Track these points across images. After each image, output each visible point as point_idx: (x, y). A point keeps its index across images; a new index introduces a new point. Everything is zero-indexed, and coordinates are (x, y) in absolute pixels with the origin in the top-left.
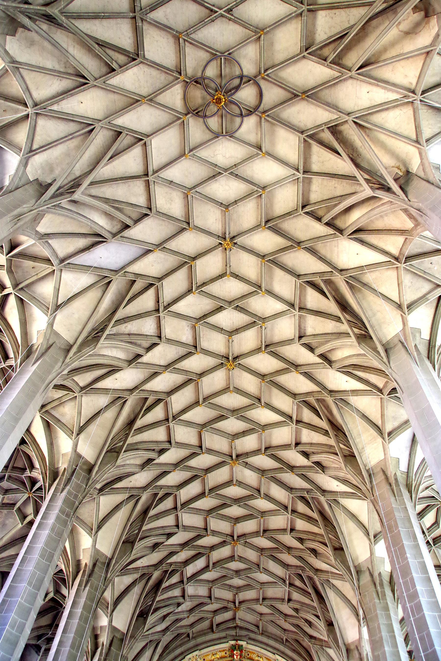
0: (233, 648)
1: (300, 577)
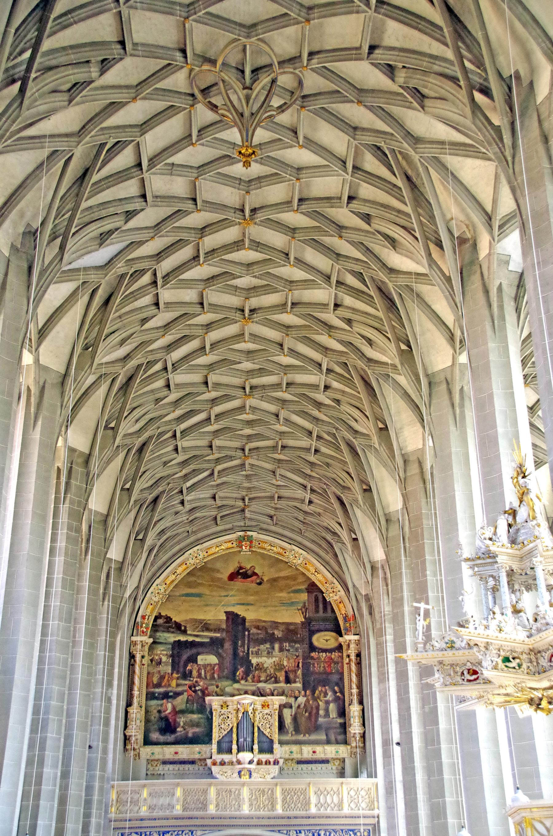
0: (240, 541)
1: (359, 276)
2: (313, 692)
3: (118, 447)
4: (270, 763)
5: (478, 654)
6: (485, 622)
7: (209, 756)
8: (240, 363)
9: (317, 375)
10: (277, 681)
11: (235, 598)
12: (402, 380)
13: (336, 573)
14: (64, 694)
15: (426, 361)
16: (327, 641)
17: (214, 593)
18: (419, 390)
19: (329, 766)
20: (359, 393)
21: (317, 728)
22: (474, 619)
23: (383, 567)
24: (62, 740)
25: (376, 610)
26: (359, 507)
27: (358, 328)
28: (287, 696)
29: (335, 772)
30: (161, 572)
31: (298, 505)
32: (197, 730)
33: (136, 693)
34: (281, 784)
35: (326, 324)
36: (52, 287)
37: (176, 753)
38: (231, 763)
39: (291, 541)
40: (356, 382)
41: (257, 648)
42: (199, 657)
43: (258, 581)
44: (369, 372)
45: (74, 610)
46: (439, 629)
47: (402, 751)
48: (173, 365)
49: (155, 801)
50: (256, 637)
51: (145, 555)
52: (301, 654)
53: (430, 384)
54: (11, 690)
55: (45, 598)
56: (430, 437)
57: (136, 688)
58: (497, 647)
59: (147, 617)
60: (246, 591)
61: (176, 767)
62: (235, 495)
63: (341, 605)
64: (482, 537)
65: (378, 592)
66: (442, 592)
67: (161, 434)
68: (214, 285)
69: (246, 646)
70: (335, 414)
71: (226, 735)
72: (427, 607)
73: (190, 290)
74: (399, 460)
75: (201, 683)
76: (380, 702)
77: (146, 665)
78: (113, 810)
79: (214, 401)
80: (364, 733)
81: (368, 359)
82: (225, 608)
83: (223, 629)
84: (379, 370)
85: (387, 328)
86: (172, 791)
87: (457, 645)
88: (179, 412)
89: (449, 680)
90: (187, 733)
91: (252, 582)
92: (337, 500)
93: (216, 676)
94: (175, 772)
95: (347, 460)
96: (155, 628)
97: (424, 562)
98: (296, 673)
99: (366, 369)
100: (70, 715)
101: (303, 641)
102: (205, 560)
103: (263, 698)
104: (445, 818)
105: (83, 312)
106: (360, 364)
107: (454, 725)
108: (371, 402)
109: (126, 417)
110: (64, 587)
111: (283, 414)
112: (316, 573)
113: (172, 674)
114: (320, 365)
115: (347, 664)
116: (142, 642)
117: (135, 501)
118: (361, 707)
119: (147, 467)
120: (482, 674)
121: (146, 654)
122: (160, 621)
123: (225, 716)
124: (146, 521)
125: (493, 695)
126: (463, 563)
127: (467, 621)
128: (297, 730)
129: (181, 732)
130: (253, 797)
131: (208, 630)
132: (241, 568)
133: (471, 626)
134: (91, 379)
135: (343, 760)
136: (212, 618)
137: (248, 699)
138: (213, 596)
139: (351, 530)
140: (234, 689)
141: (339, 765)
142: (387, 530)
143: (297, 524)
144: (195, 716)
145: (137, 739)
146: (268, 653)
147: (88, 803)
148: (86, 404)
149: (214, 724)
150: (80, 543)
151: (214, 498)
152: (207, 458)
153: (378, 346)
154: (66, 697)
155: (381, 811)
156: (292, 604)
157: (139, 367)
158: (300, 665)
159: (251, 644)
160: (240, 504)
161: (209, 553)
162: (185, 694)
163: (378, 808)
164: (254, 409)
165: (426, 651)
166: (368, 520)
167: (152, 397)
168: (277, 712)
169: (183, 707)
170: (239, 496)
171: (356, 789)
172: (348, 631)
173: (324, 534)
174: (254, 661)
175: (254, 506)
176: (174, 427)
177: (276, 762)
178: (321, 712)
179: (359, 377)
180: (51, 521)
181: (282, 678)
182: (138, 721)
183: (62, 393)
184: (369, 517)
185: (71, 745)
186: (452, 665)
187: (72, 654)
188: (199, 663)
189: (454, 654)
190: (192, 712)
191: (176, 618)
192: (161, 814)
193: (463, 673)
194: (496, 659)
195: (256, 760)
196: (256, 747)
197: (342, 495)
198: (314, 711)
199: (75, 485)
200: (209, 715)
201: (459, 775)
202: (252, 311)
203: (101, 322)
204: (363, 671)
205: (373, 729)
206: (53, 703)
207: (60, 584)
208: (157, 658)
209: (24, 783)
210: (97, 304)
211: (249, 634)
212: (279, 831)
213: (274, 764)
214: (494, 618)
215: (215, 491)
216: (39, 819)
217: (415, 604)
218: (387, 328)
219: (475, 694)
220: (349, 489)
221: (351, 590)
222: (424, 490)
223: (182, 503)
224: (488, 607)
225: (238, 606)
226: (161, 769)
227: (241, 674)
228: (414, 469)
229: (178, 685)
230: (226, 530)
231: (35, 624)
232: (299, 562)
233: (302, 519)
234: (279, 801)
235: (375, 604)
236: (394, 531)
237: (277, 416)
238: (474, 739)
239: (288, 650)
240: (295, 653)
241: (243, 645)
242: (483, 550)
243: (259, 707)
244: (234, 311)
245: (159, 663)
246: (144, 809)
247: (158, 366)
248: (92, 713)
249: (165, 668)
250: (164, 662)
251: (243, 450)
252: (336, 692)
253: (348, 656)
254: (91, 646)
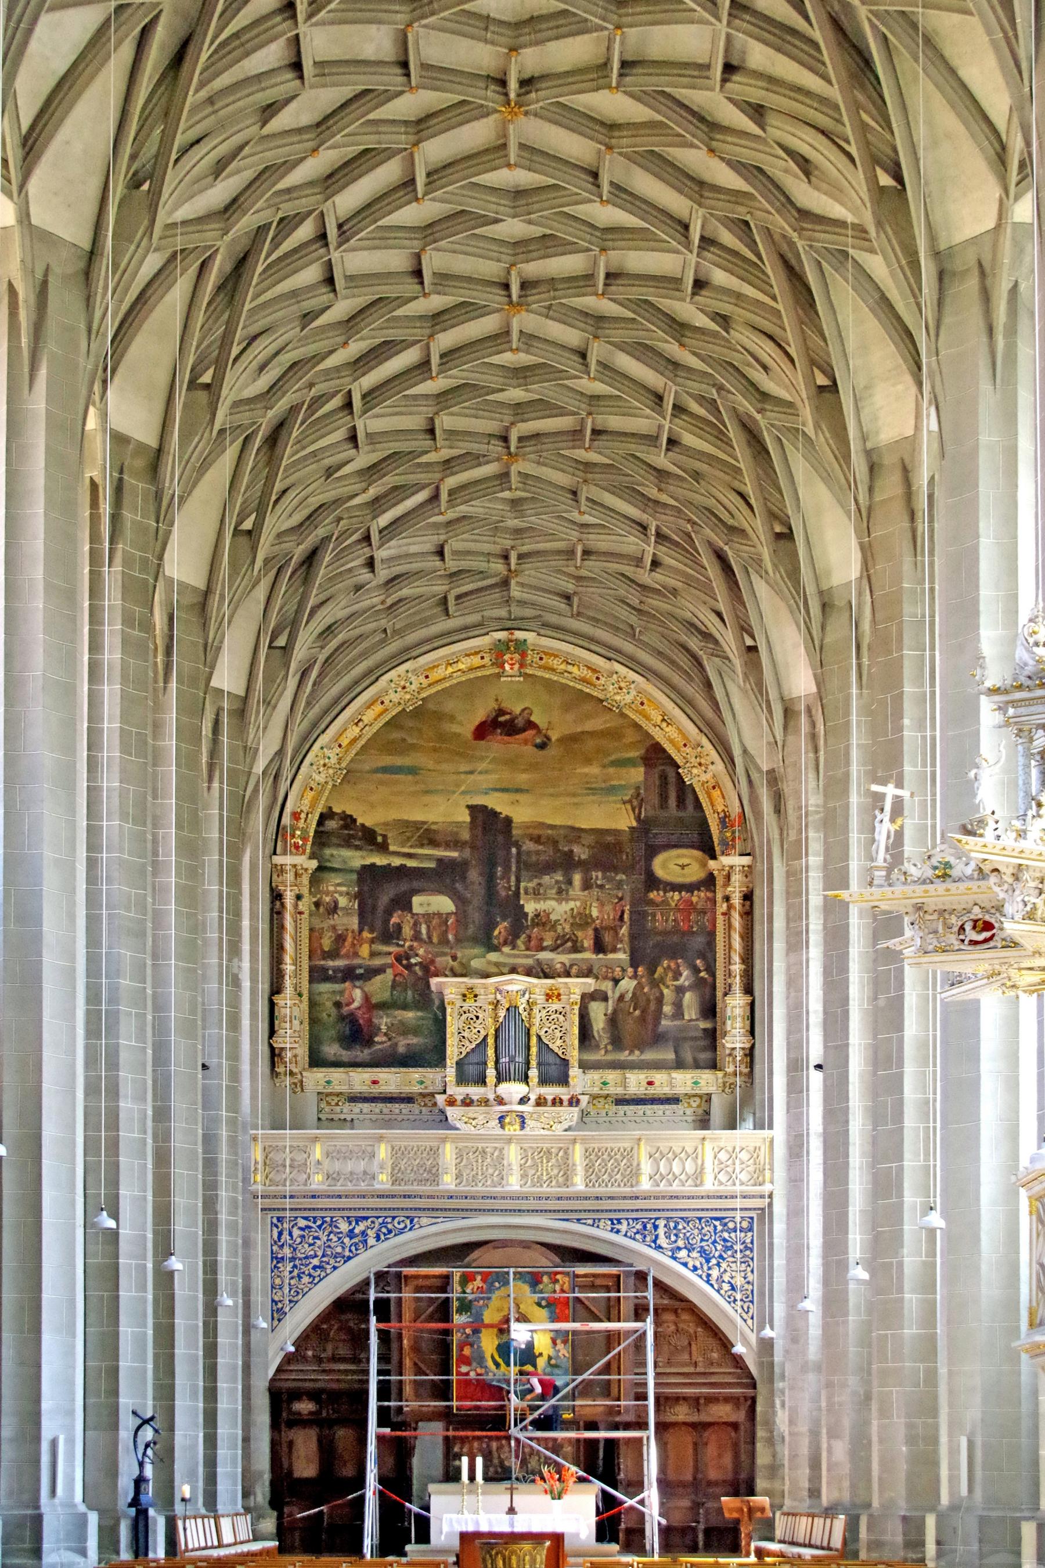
0: (500, 650)
2: (652, 971)
3: (222, 431)
4: (561, 1102)
5: (997, 889)
6: (1018, 824)
7: (440, 1089)
8: (497, 221)
9: (677, 252)
10: (576, 949)
12: (877, 265)
13: (709, 724)
14: (145, 964)
15: (937, 217)
16: (683, 867)
17: (445, 766)
18: (915, 292)
19: (679, 1108)
20: (774, 298)
21: (658, 1039)
22: (996, 817)
23: (809, 710)
24: (150, 1052)
25: (791, 804)
26: (763, 574)
27: (779, 130)
28: (597, 978)
29: (690, 1119)
30: (329, 719)
31: (629, 570)
32: (414, 1040)
33: (288, 968)
34: (584, 1140)
35: (702, 119)
36: (45, 19)
37: (375, 1082)
38: (485, 1102)
39: (612, 653)
40: (769, 271)
41: (536, 881)
42: (416, 900)
43: (538, 741)
44: (800, 244)
45: (149, 798)
46: (921, 841)
47: (825, 1080)
48: (340, 226)
49: (337, 1166)
50: (534, 858)
51: (292, 683)
53: (941, 275)
54: (40, 954)
55: (89, 771)
56: (933, 410)
57: (288, 959)
58: (1038, 875)
59: (303, 816)
60: (510, 763)
61: (378, 1107)
62: (487, 548)
63: (716, 793)
64: (1031, 640)
65: (796, 765)
66: (933, 765)
67: (317, 401)
68: (433, 14)
69: (513, 878)
70: (718, 351)
71: (473, 1050)
72: (899, 792)
73: (374, 27)
74: (859, 465)
75: (421, 952)
76: (788, 989)
77: (307, 912)
78: (259, 1178)
79: (438, 320)
80: (752, 1047)
81: (799, 211)
82: (468, 797)
83: (465, 843)
84: (826, 238)
85: (848, 131)
86: (369, 1149)
87: (955, 873)
88: (356, 347)
89: (932, 942)
90: (396, 1044)
91: (526, 742)
92: (714, 559)
93: (450, 937)
94: (374, 1117)
95: (742, 466)
96: (322, 838)
97: (899, 699)
98: (617, 933)
99: (794, 235)
100: (160, 1006)
101: (633, 867)
102: (424, 695)
103: (549, 982)
104: (900, 1195)
105: (123, 87)
106: (781, 223)
107: (935, 1030)
108: (802, 323)
109: (236, 360)
110: (125, 749)
111: (597, 351)
112: (664, 725)
113: (361, 931)
114: (686, 227)
115: (723, 914)
116: (295, 866)
117: (267, 561)
118: (749, 999)
119: (288, 482)
120: (1002, 929)
121: (305, 891)
122: (332, 825)
123: (471, 1016)
124: (292, 607)
125: (1020, 969)
126: (983, 698)
127: (982, 822)
128: (617, 1042)
129: (382, 1043)
130: (529, 1163)
131: (433, 843)
132: (501, 712)
133: (989, 833)
134: (152, 263)
135: (708, 1098)
136: (441, 819)
137: (517, 983)
138: (443, 773)
139: (745, 629)
140: (489, 963)
141: (699, 1106)
142: (823, 628)
143: (623, 613)
144: (410, 1015)
145: (295, 1056)
146: (560, 892)
147: (210, 1165)
148: (146, 326)
149: (449, 1030)
150: (151, 654)
151: (440, 553)
152: (424, 459)
153: (825, 178)
154: (149, 971)
155: (778, 1186)
156: (611, 790)
157: (262, 230)
158: (626, 917)
159: (524, 873)
160: (499, 567)
161: (431, 680)
162: (389, 971)
163: (772, 1182)
164: (529, 339)
165: (890, 885)
166: (782, 605)
167: (295, 310)
168: (577, 1007)
169: (385, 996)
170: (497, 549)
171: (730, 1149)
172: (728, 847)
173: (684, 638)
174: (530, 907)
175: (531, 573)
176: (344, 382)
177: (574, 1102)
178: (667, 1009)
179: (776, 257)
180: (87, 604)
181: (588, 943)
182: (296, 1023)
183: (89, 301)
184: (783, 598)
185: (166, 1063)
186: (942, 912)
187: (154, 888)
188: (415, 911)
189: (948, 890)
190: (405, 1007)
191: (365, 818)
192: (350, 1187)
193: (962, 928)
194: (1033, 900)
195: (533, 1097)
196: (533, 1073)
197: (726, 548)
198: (653, 1006)
199: (133, 522)
200: (439, 1014)
201: (935, 1121)
202: (527, 83)
203: (166, 114)
204: (757, 928)
205: (771, 1046)
206: (125, 982)
207: (117, 742)
208: (327, 899)
209: (85, 1124)
210: (154, 68)
211: (519, 853)
212: (578, 1220)
213: (570, 1104)
214: (1039, 816)
215: (443, 537)
216: (121, 1187)
217: (875, 788)
218: (848, 131)
219: (983, 968)
220: (742, 532)
221: (738, 760)
222: (909, 535)
223: (370, 564)
224: (1027, 793)
226: (349, 1110)
227: (503, 933)
228: (890, 486)
229: (373, 954)
230: (466, 628)
231: (72, 825)
232: (628, 699)
233: (635, 602)
234: (580, 1170)
235: (787, 788)
236: (838, 630)
237: (583, 355)
238: (973, 1056)
239: (601, 887)
241: (506, 876)
242: (1029, 670)
243: (540, 999)
244: (482, 85)
245: (334, 909)
246: (319, 1178)
247: (305, 231)
248: (203, 1004)
249: (345, 920)
250: (343, 909)
251: (505, 439)
252: (696, 970)
253: (727, 899)
254: (192, 872)
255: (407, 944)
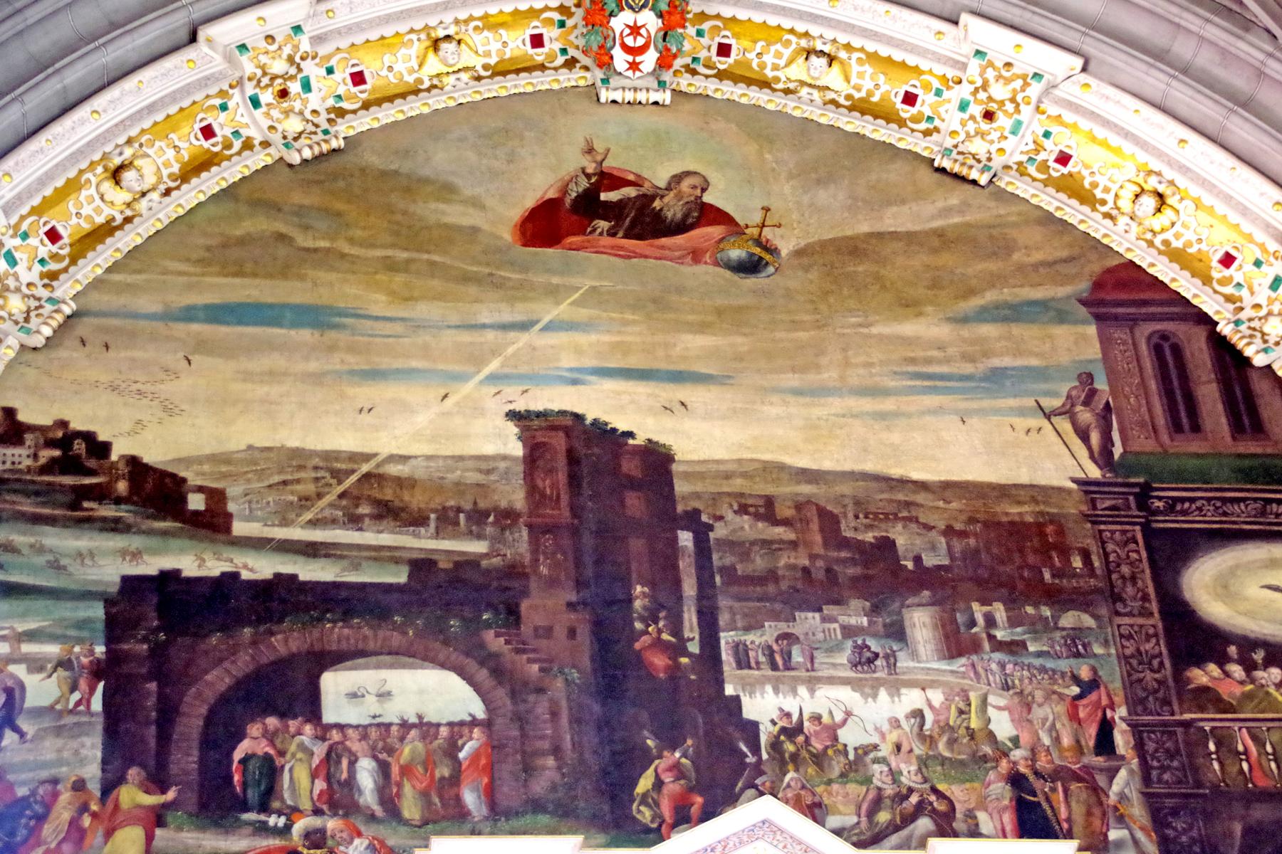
11: (581, 339)
42: (334, 683)
43: (736, 254)
50: (759, 563)
52: (1113, 678)
69: (690, 618)
82: (511, 391)
91: (696, 256)
93: (470, 798)
98: (1097, 792)
113: (109, 788)
131: (389, 512)
158: (1122, 740)
188: (329, 717)
225: (610, 385)
232: (1015, 149)
239: (1013, 648)
240: (1064, 665)
250: (39, 712)
255: (299, 826)
